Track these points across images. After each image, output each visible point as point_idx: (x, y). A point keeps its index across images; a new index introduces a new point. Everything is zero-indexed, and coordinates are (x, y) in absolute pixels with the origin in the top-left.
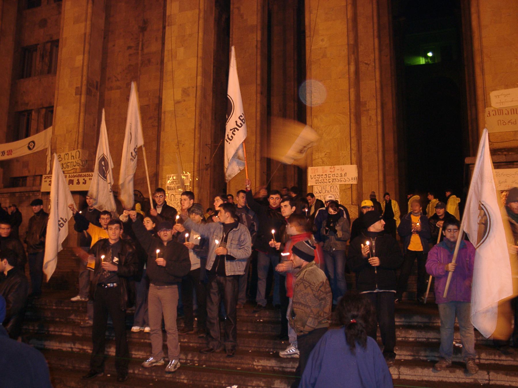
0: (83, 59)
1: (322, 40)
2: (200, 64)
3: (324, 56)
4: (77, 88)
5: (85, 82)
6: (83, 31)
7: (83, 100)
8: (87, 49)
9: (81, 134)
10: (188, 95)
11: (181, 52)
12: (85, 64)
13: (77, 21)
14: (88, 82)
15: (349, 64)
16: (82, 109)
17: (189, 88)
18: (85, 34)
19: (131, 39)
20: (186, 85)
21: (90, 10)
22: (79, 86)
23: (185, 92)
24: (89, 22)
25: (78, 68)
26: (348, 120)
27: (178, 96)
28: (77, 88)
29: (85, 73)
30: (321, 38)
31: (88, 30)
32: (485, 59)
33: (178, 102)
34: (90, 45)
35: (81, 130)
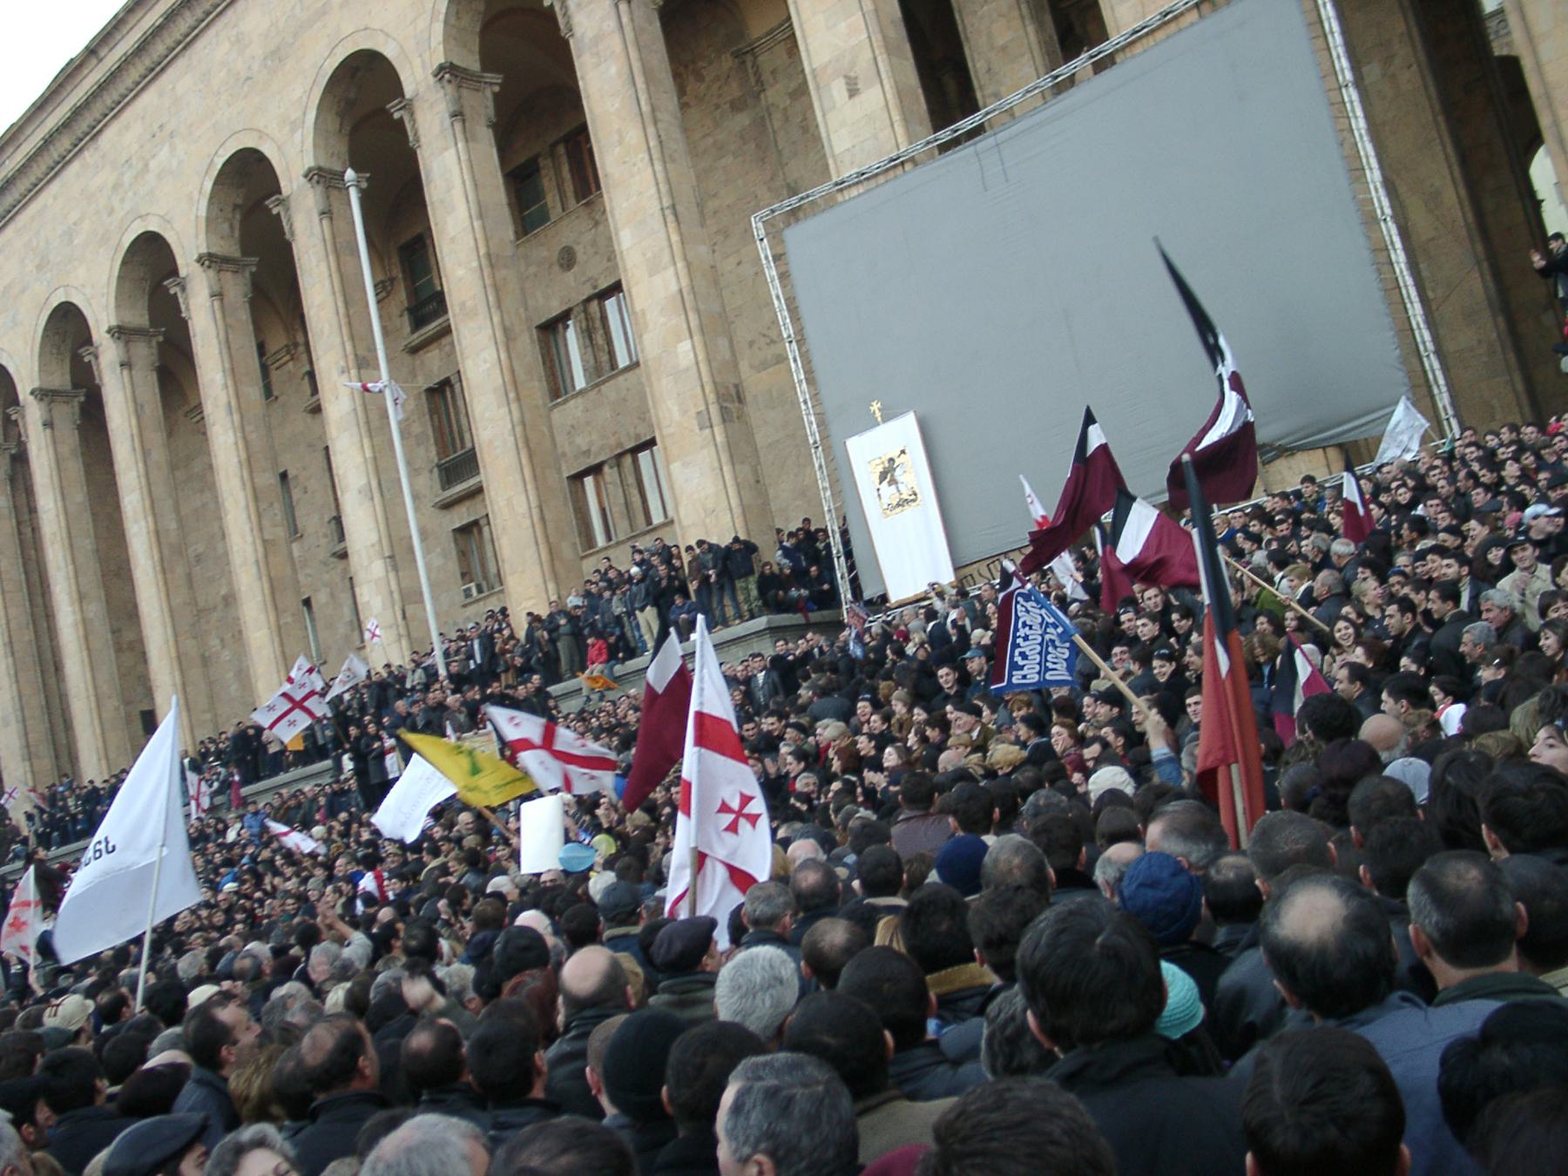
0: (694, 348)
4: (699, 413)
5: (712, 397)
6: (674, 288)
7: (720, 438)
8: (694, 322)
9: (737, 511)
12: (701, 357)
13: (654, 270)
14: (717, 394)
16: (724, 457)
18: (681, 291)
21: (675, 238)
22: (703, 408)
24: (680, 265)
25: (687, 369)
29: (706, 378)
31: (685, 282)
34: (698, 311)
35: (734, 502)
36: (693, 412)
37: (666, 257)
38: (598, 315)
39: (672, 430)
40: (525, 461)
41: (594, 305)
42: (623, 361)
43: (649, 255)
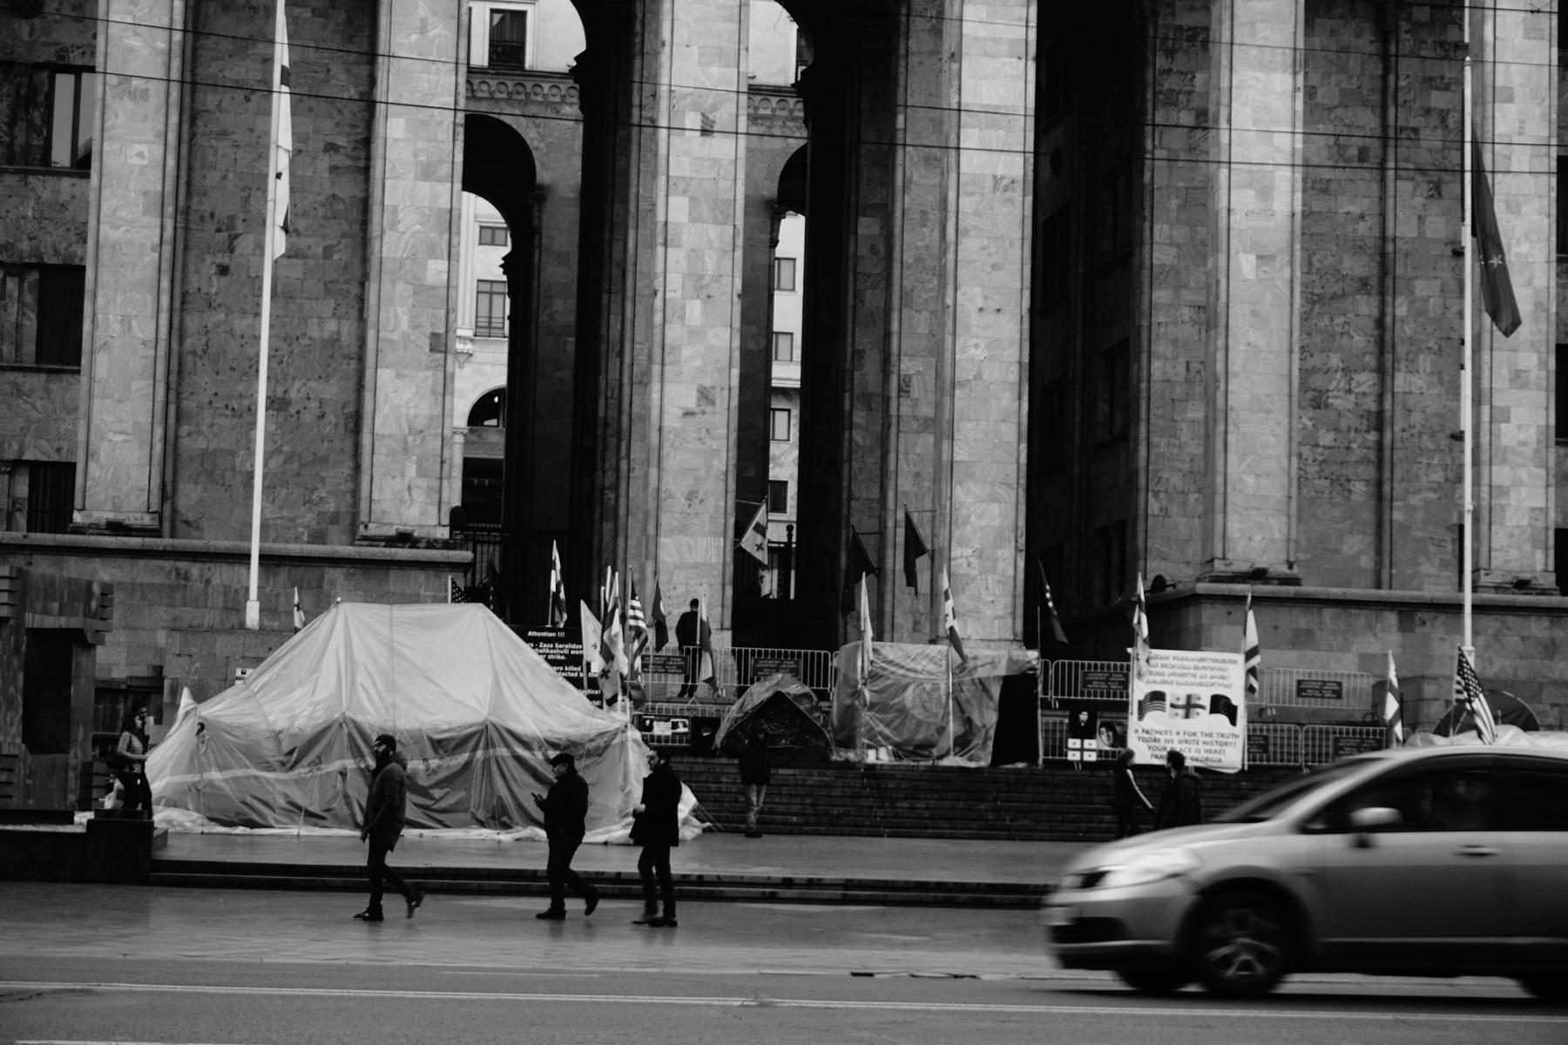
1: (976, 346)
2: (737, 343)
3: (978, 376)
4: (434, 336)
10: (713, 403)
11: (695, 309)
15: (1020, 398)
17: (713, 388)
19: (337, 125)
20: (707, 382)
22: (442, 331)
23: (705, 395)
25: (434, 288)
26: (1014, 496)
27: (691, 404)
28: (434, 336)
30: (974, 341)
32: (1231, 428)
33: (688, 414)
36: (428, 331)
37: (445, 169)
38: (46, 88)
39: (395, 336)
40: (165, 284)
41: (44, 76)
42: (61, 155)
43: (422, 158)
